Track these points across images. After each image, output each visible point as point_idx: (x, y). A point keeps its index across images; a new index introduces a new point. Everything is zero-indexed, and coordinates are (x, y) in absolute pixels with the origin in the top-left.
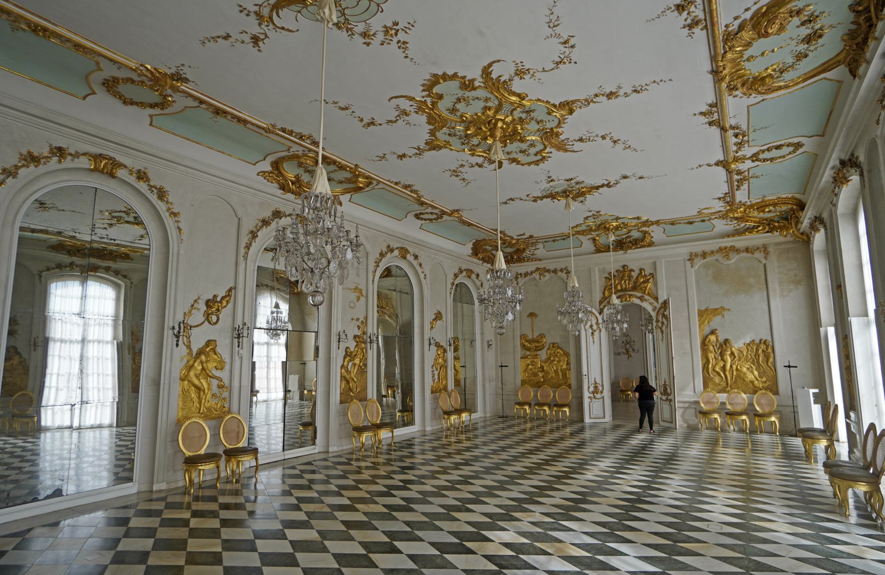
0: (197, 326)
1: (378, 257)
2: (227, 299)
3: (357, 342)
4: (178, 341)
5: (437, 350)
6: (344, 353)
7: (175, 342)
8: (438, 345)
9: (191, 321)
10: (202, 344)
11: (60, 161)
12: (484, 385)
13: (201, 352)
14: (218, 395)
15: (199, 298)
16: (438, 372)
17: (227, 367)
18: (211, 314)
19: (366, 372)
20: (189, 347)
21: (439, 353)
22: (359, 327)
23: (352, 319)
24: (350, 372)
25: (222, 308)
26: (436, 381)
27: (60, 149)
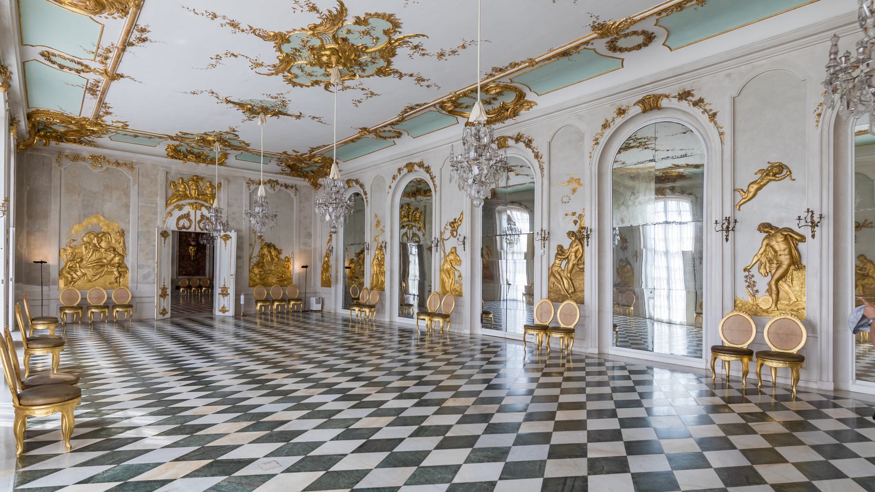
8: (766, 228)
20: (444, 252)
22: (575, 222)
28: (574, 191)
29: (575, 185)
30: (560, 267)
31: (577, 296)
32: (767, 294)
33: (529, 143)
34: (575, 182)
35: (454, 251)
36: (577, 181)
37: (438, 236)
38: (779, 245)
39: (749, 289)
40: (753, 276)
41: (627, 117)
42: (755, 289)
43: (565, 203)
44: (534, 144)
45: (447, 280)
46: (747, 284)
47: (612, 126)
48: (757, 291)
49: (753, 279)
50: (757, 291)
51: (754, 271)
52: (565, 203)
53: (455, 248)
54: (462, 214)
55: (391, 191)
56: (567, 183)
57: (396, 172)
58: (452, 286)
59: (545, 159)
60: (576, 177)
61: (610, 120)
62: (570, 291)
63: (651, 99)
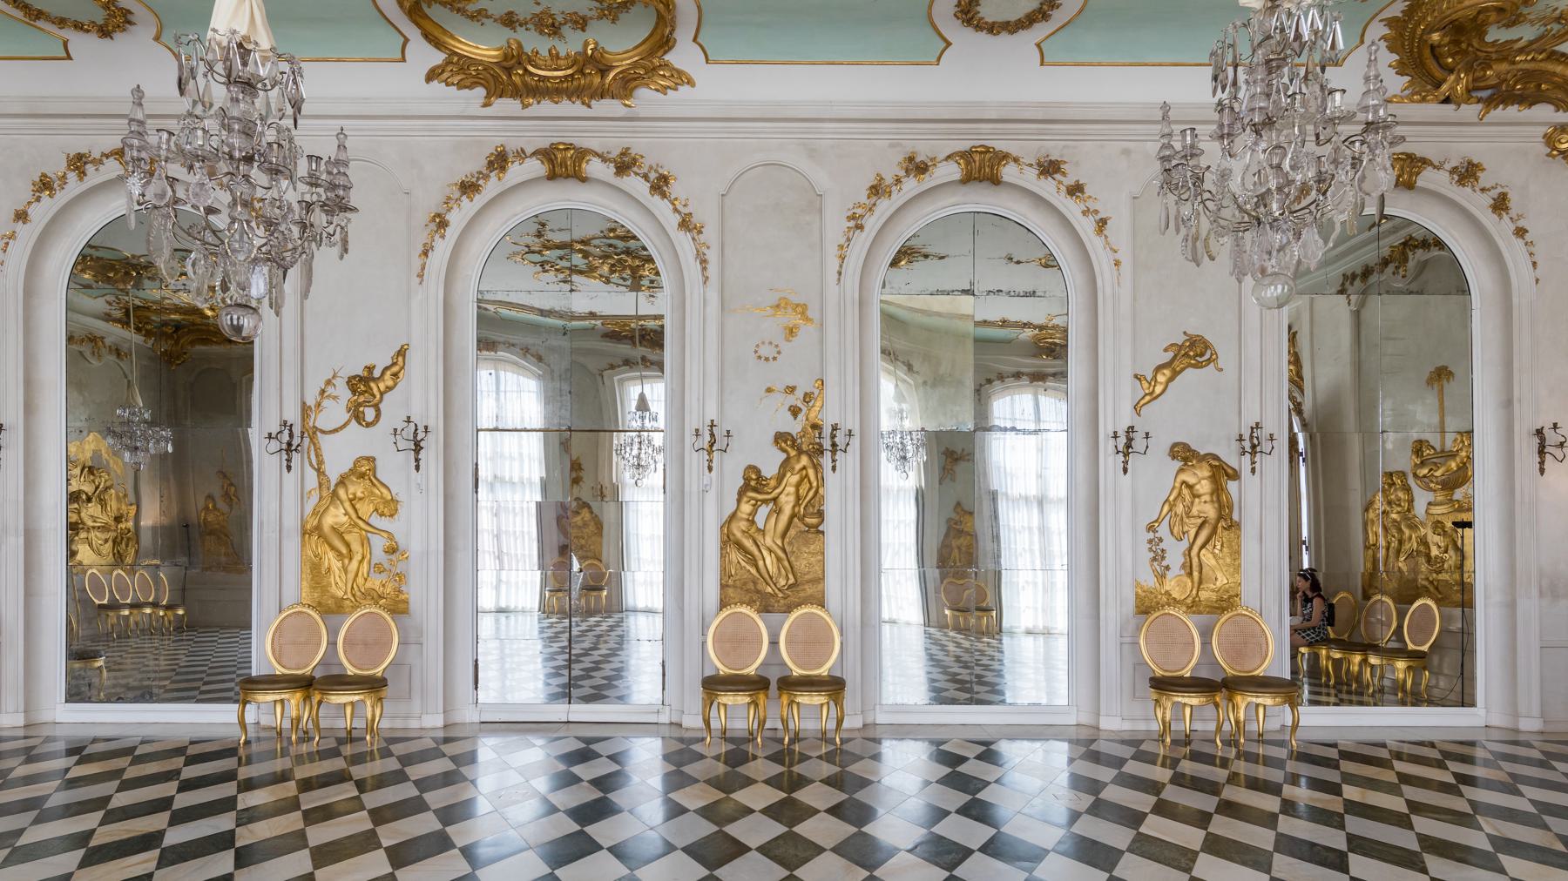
0: (336, 431)
1: (863, 198)
2: (395, 369)
3: (784, 451)
4: (289, 460)
5: (1181, 470)
6: (742, 482)
7: (285, 463)
8: (1183, 454)
9: (323, 420)
10: (346, 466)
11: (81, 179)
12: (1511, 606)
13: (342, 482)
14: (386, 566)
15: (334, 377)
16: (1185, 544)
17: (402, 511)
18: (360, 405)
19: (823, 533)
21: (1191, 480)
22: (795, 411)
23: (769, 390)
24: (763, 532)
25: (382, 394)
26: (1169, 575)
27: (80, 157)
28: (791, 332)
29: (795, 319)
30: (752, 522)
31: (802, 594)
32: (1183, 572)
33: (660, 185)
34: (795, 310)
35: (365, 470)
36: (799, 309)
37: (292, 415)
38: (1200, 479)
39: (1155, 563)
40: (1161, 540)
41: (928, 181)
42: (1164, 563)
43: (767, 359)
44: (675, 189)
45: (336, 565)
46: (1152, 555)
47: (894, 196)
48: (1167, 568)
49: (1162, 546)
50: (1167, 568)
51: (1163, 530)
52: (767, 359)
53: (371, 460)
54: (402, 352)
55: (27, 234)
56: (769, 311)
57: (57, 167)
58: (360, 580)
59: (710, 235)
60: (795, 299)
61: (889, 180)
62: (782, 582)
63: (988, 156)
